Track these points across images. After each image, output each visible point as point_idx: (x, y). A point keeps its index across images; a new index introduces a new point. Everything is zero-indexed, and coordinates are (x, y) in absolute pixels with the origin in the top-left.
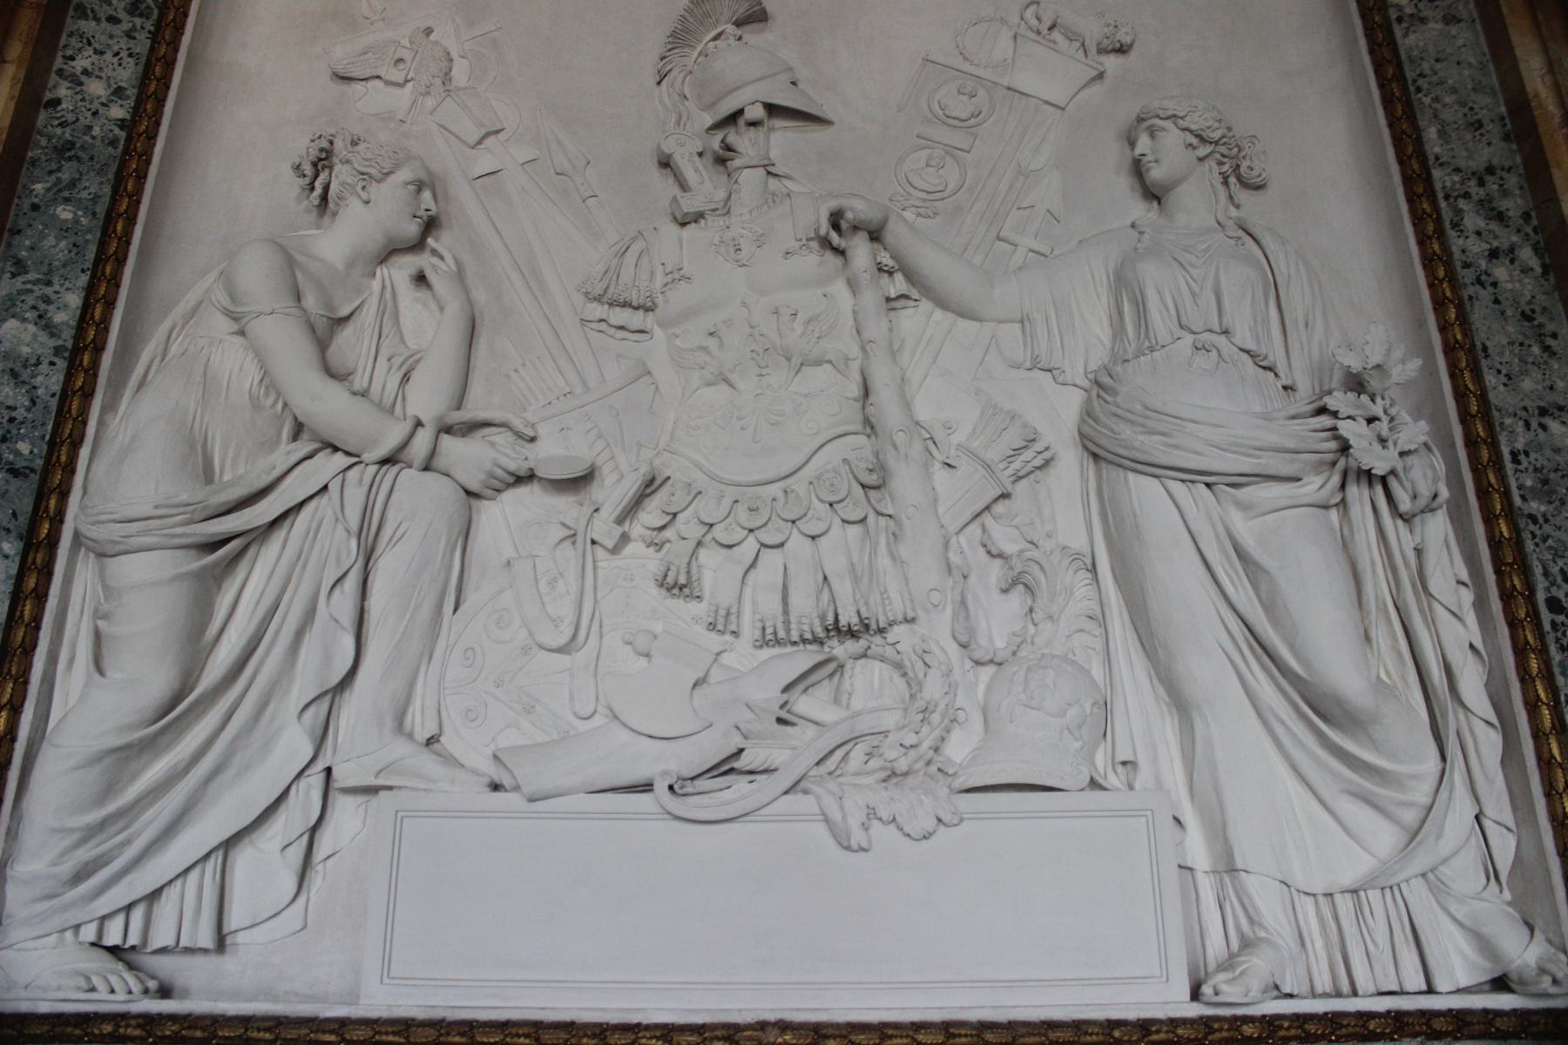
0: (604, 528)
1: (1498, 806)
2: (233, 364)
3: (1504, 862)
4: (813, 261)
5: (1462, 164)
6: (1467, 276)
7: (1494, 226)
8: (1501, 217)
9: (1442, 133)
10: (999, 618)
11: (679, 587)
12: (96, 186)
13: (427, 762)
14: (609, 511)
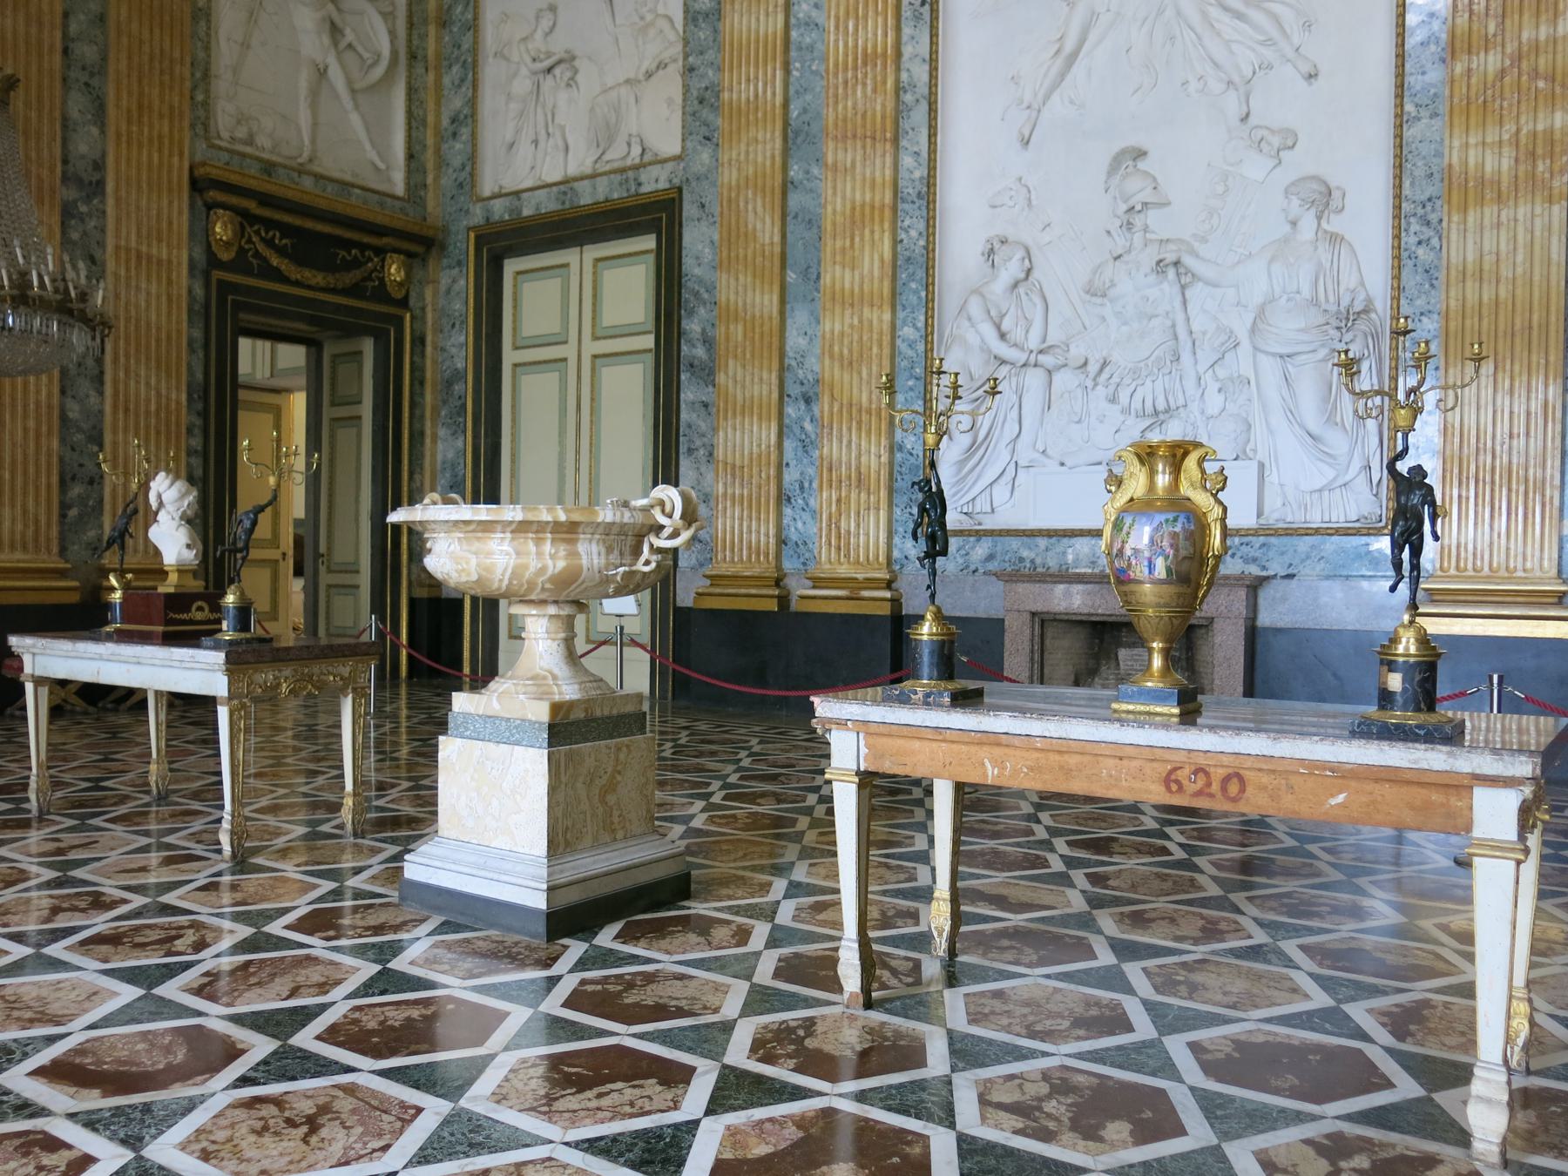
0: (1089, 383)
1: (1376, 465)
2: (972, 338)
3: (1375, 481)
4: (1153, 278)
5: (1416, 198)
6: (1405, 255)
7: (1424, 229)
8: (1428, 223)
9: (1412, 184)
10: (1215, 402)
11: (1113, 400)
12: (921, 274)
13: (1042, 458)
14: (1092, 375)
